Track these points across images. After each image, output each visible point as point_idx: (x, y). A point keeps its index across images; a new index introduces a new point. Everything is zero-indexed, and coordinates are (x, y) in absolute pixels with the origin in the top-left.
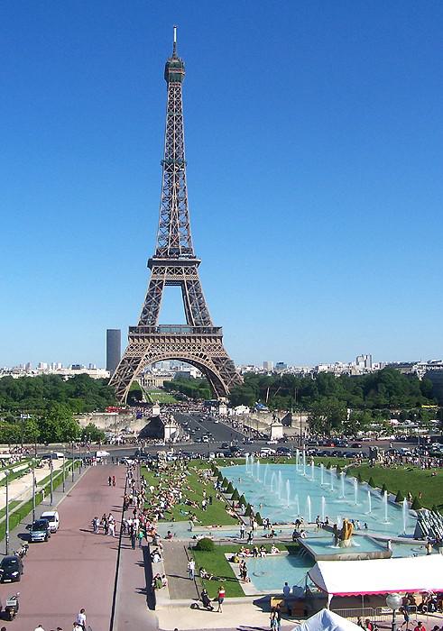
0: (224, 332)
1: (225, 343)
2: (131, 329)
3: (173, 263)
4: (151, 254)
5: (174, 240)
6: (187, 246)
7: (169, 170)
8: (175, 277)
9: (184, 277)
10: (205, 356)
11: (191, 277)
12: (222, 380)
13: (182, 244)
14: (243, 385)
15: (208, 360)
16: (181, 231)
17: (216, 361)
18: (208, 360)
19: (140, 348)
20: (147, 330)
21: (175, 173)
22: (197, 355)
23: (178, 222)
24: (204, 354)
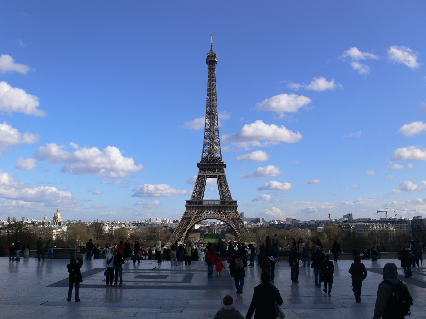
0: (238, 204)
1: (240, 210)
3: (210, 165)
4: (199, 160)
6: (219, 156)
7: (209, 114)
12: (237, 230)
13: (217, 155)
18: (229, 219)
19: (192, 212)
24: (227, 216)
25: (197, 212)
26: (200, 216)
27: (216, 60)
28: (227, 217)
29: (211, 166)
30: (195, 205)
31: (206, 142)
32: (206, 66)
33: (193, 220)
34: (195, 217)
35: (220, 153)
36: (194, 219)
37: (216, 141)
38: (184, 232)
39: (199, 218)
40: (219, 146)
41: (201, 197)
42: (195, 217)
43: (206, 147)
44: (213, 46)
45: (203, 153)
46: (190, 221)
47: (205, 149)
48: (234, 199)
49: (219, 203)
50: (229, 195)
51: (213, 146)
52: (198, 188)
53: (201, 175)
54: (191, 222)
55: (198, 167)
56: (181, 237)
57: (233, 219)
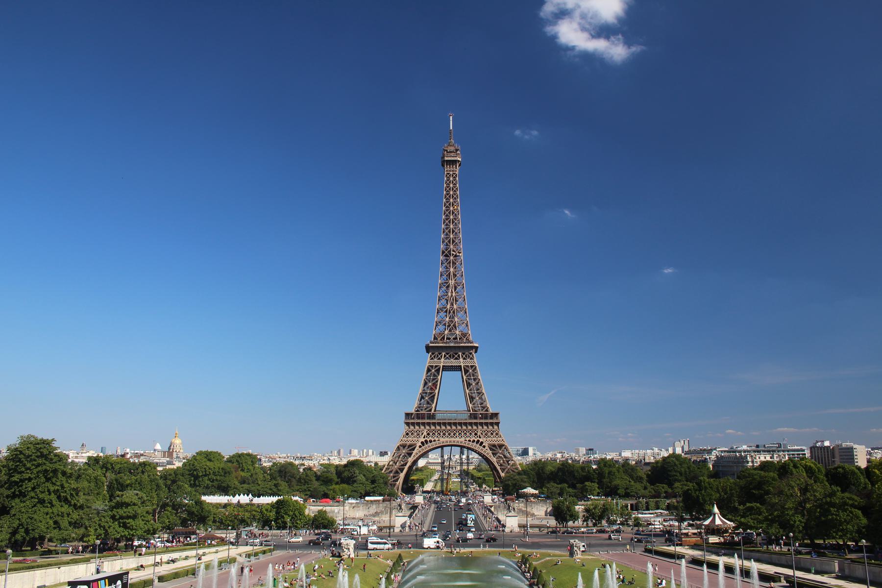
0: (501, 418)
2: (408, 415)
5: (452, 327)
7: (446, 256)
8: (453, 362)
9: (462, 362)
10: (482, 443)
11: (468, 362)
12: (498, 468)
14: (519, 473)
15: (484, 447)
17: (493, 447)
18: (484, 447)
20: (422, 417)
21: (452, 258)
22: (474, 441)
23: (455, 307)
24: (481, 440)
25: (425, 433)
26: (431, 441)
28: (482, 443)
29: (450, 350)
33: (417, 447)
34: (422, 443)
36: (420, 447)
38: (402, 470)
39: (429, 444)
42: (422, 443)
46: (413, 449)
49: (464, 417)
53: (432, 366)
54: (414, 452)
55: (428, 352)
56: (397, 480)
57: (493, 447)
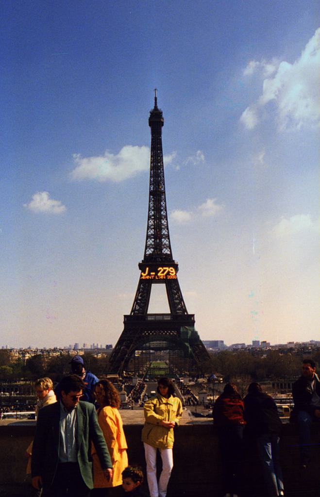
1: (197, 327)
2: (125, 316)
4: (141, 258)
6: (169, 253)
13: (166, 251)
16: (165, 241)
27: (162, 120)
30: (138, 323)
31: (149, 233)
32: (149, 130)
35: (170, 248)
37: (164, 232)
40: (169, 239)
41: (145, 311)
43: (151, 242)
44: (158, 101)
45: (146, 247)
47: (149, 243)
48: (190, 313)
49: (169, 318)
50: (182, 307)
51: (160, 240)
52: (139, 298)
55: (140, 269)
